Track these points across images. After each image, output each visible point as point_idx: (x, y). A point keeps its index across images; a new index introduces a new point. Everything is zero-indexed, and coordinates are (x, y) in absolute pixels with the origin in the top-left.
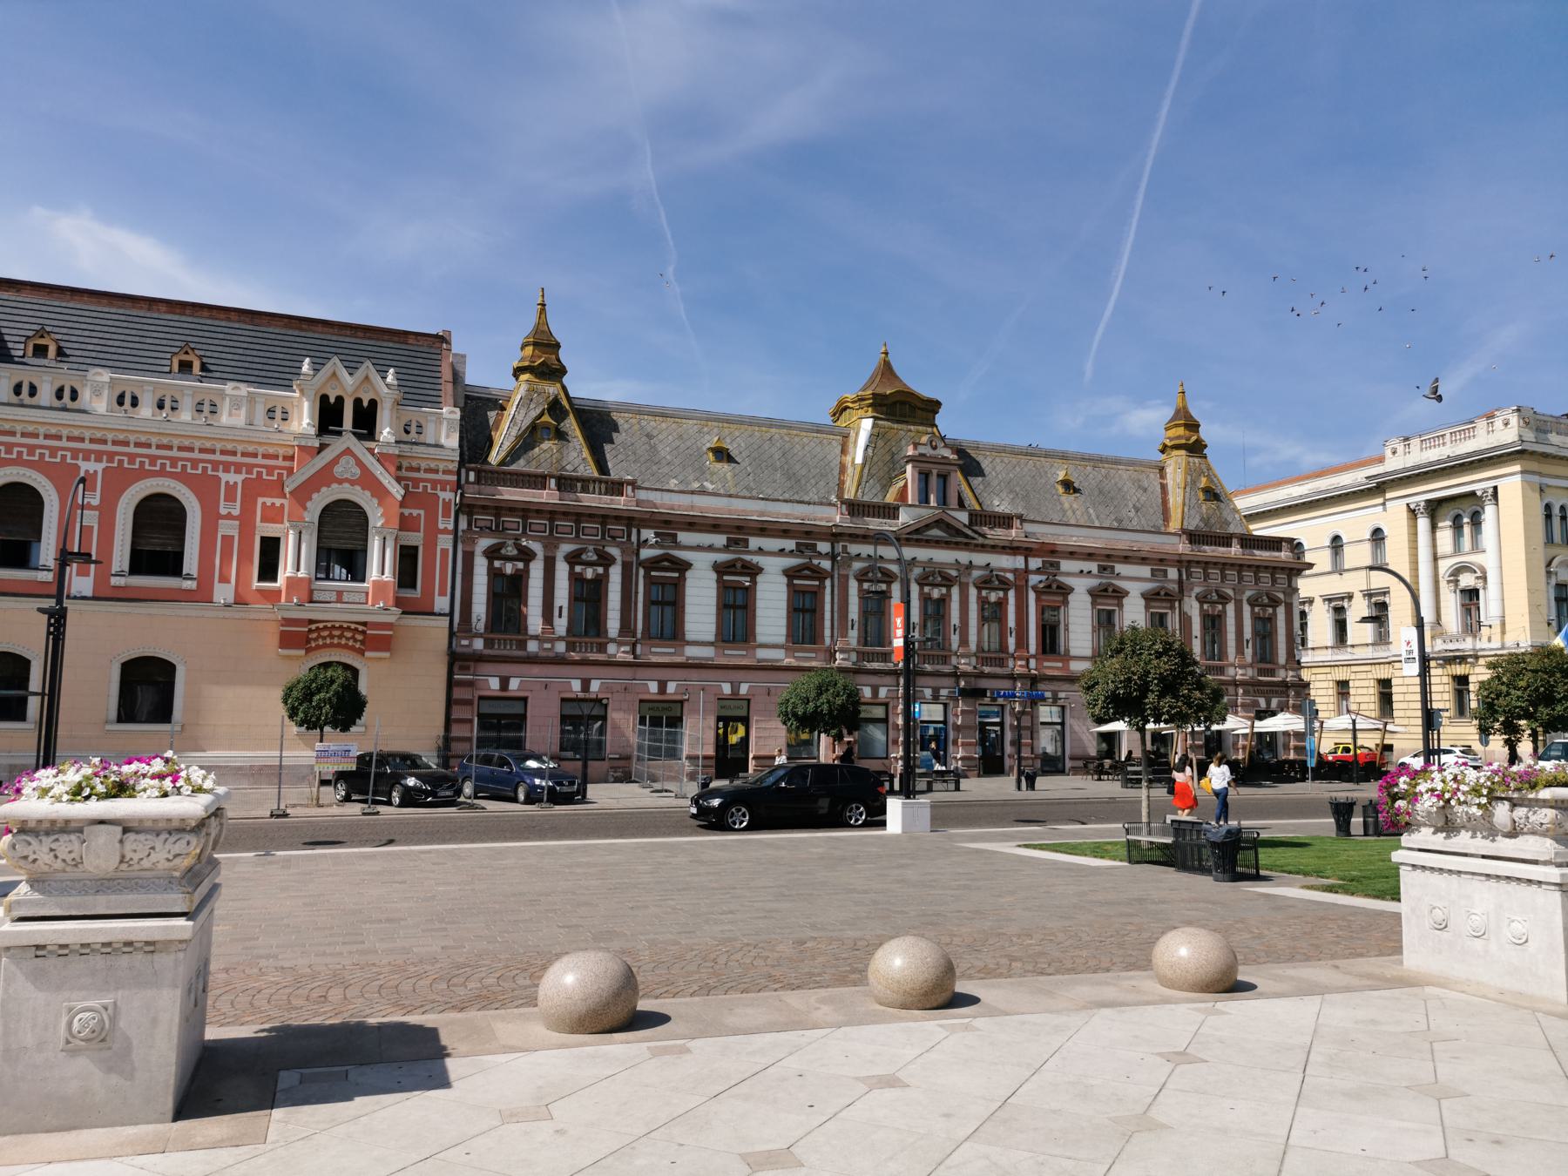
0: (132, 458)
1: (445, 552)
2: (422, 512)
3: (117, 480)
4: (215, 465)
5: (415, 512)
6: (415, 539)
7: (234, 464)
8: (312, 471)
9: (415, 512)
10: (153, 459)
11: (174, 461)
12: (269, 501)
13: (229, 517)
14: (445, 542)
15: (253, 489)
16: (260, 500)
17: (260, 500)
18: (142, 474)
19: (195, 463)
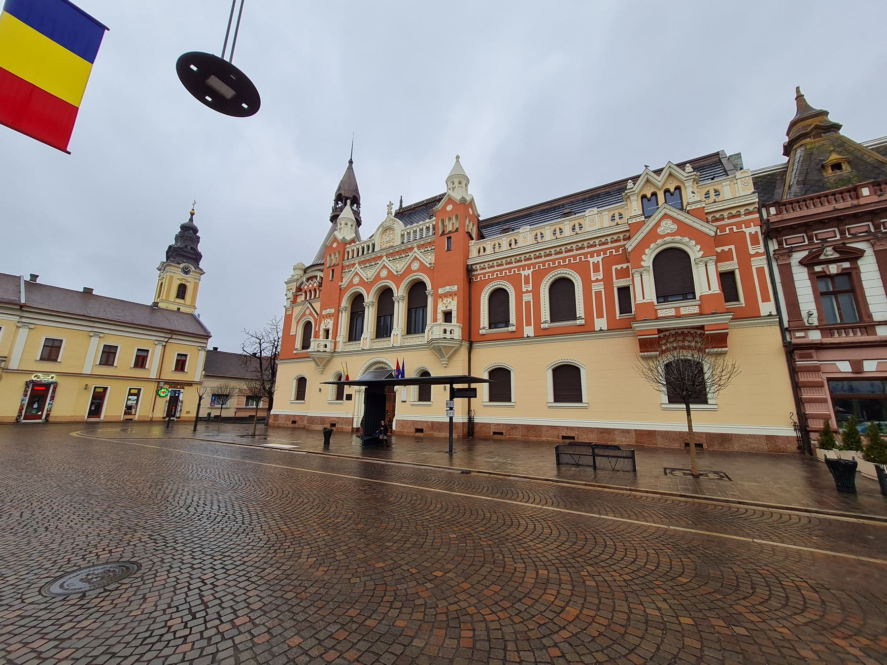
0: (544, 263)
1: (760, 270)
2: (733, 247)
3: (538, 276)
4: (586, 255)
5: (726, 248)
6: (731, 265)
7: (595, 252)
8: (642, 235)
9: (726, 248)
10: (554, 261)
11: (564, 259)
12: (619, 267)
13: (597, 280)
14: (759, 262)
15: (608, 263)
18: (550, 269)
19: (574, 257)
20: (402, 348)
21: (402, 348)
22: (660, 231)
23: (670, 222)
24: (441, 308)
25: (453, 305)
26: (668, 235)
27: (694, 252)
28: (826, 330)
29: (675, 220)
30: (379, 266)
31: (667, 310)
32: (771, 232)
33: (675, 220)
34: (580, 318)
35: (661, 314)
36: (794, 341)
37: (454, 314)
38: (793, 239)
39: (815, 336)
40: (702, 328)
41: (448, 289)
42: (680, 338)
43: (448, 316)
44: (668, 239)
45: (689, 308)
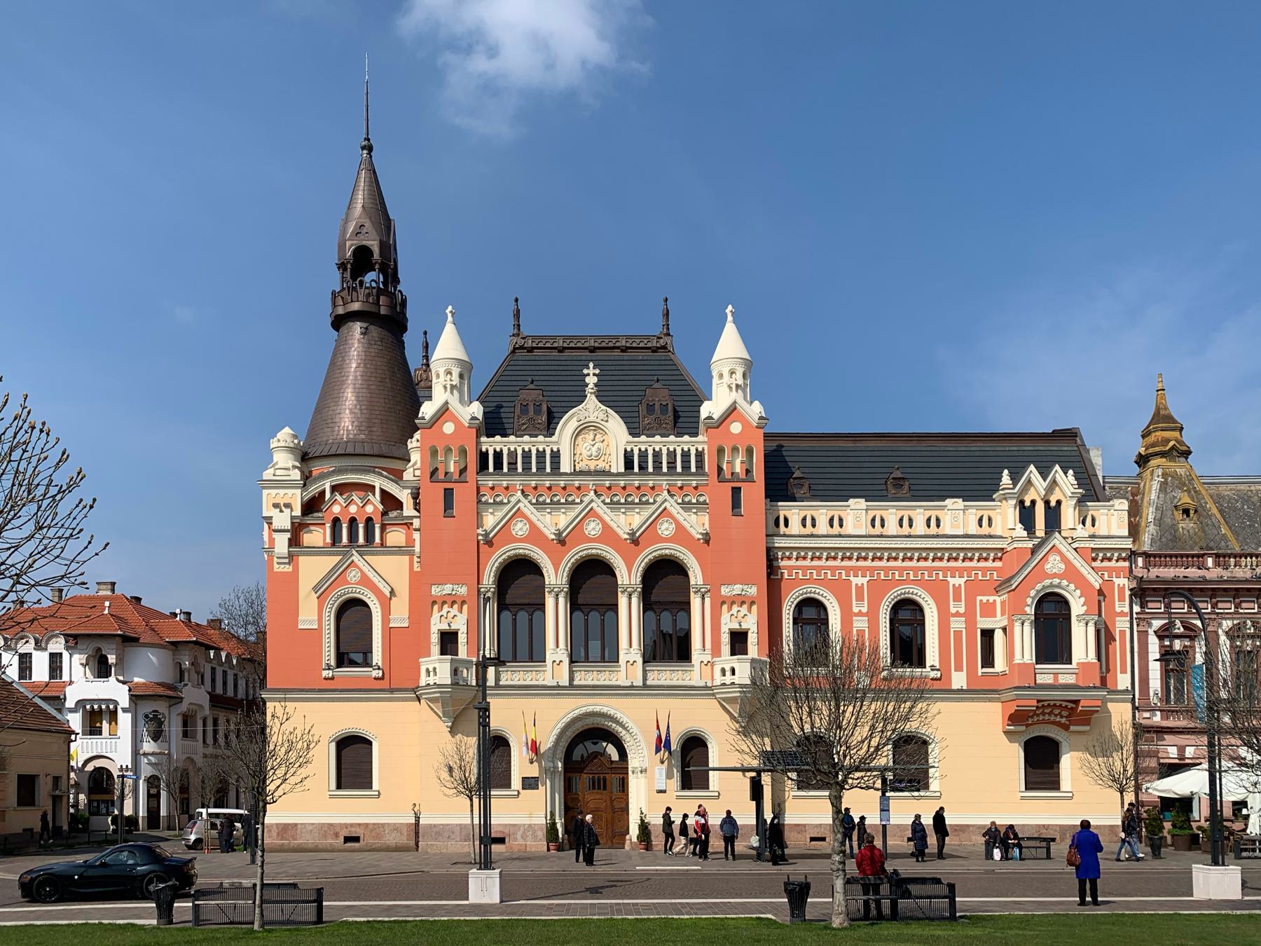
16: (979, 598)
17: (979, 598)
20: (628, 691)
21: (628, 691)
22: (1048, 566)
23: (1058, 558)
24: (728, 623)
25: (751, 621)
26: (1055, 575)
27: (1077, 607)
28: (1166, 713)
29: (1064, 559)
31: (1047, 674)
32: (1142, 592)
33: (1064, 559)
34: (933, 668)
35: (1041, 679)
36: (1144, 722)
37: (752, 639)
38: (1157, 606)
39: (1157, 718)
40: (1076, 702)
41: (737, 589)
42: (1057, 712)
43: (738, 641)
44: (1056, 581)
45: (1064, 675)
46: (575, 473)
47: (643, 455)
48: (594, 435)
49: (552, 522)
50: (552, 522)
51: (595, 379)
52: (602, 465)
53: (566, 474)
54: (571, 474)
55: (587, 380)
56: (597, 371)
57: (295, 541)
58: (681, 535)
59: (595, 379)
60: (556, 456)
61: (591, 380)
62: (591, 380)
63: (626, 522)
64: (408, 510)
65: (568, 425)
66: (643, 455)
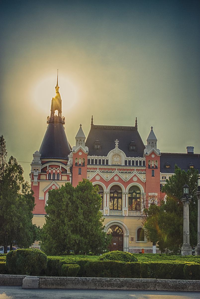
30: (114, 174)
46: (112, 165)
47: (130, 161)
48: (117, 156)
49: (107, 176)
50: (107, 176)
51: (118, 143)
52: (119, 164)
53: (110, 165)
54: (111, 165)
55: (116, 143)
56: (118, 141)
57: (39, 179)
58: (139, 181)
59: (118, 143)
60: (107, 161)
61: (117, 144)
62: (117, 144)
63: (126, 177)
64: (68, 172)
65: (110, 155)
66: (130, 161)
